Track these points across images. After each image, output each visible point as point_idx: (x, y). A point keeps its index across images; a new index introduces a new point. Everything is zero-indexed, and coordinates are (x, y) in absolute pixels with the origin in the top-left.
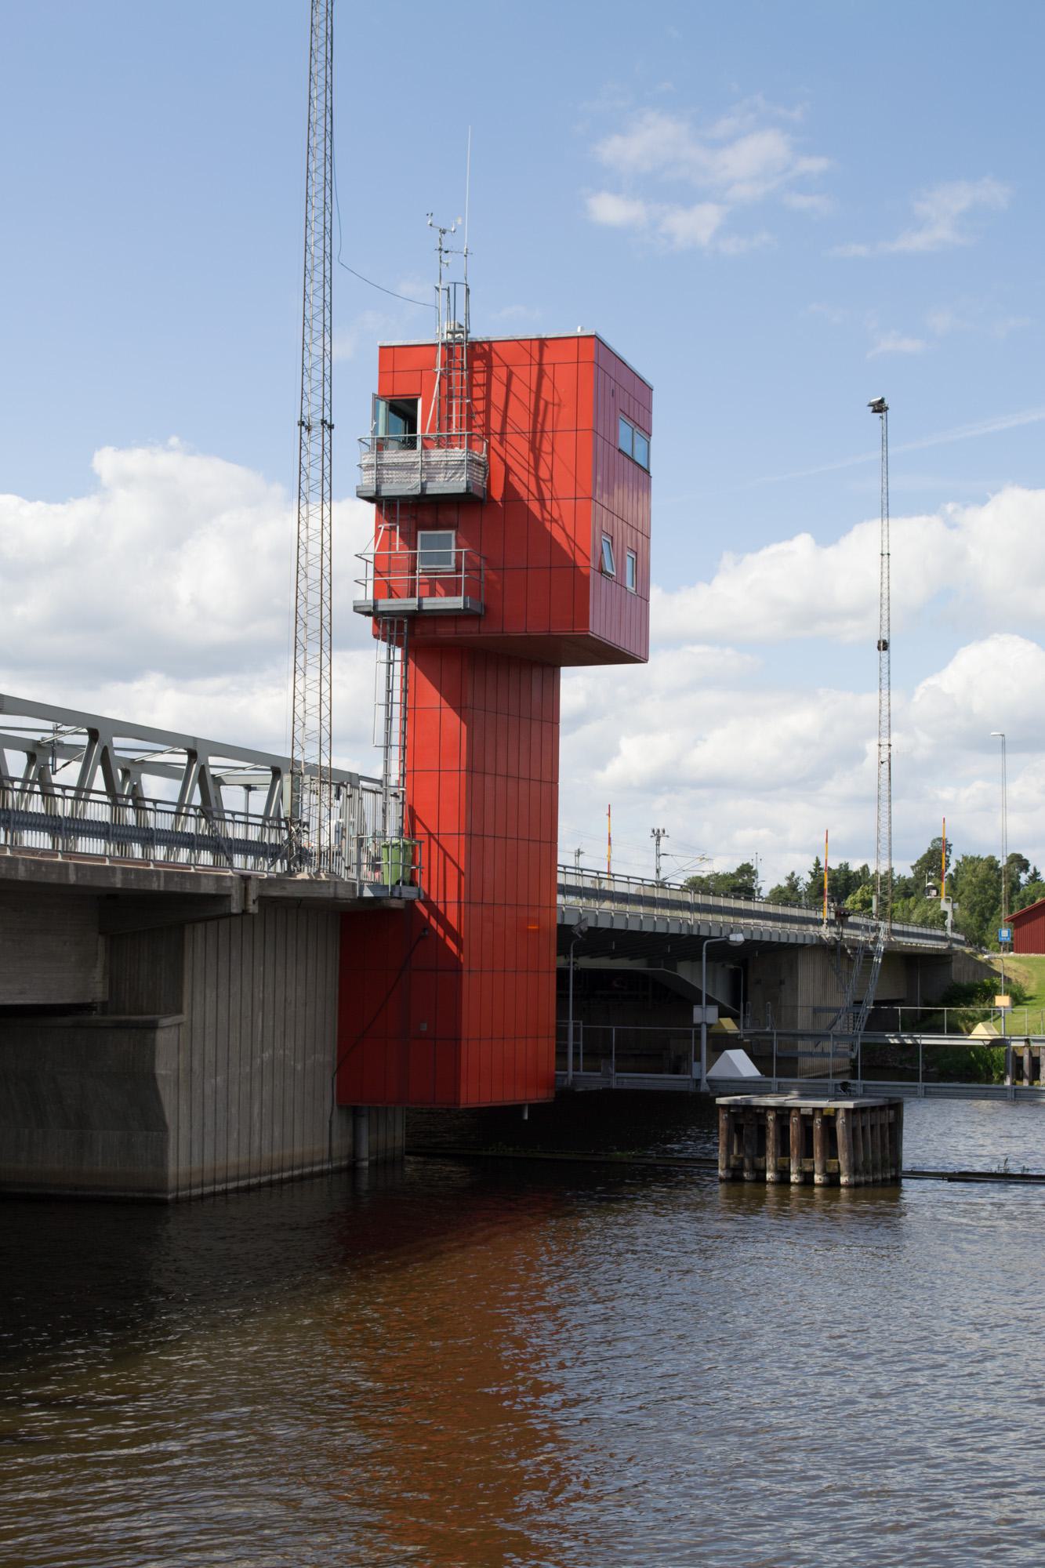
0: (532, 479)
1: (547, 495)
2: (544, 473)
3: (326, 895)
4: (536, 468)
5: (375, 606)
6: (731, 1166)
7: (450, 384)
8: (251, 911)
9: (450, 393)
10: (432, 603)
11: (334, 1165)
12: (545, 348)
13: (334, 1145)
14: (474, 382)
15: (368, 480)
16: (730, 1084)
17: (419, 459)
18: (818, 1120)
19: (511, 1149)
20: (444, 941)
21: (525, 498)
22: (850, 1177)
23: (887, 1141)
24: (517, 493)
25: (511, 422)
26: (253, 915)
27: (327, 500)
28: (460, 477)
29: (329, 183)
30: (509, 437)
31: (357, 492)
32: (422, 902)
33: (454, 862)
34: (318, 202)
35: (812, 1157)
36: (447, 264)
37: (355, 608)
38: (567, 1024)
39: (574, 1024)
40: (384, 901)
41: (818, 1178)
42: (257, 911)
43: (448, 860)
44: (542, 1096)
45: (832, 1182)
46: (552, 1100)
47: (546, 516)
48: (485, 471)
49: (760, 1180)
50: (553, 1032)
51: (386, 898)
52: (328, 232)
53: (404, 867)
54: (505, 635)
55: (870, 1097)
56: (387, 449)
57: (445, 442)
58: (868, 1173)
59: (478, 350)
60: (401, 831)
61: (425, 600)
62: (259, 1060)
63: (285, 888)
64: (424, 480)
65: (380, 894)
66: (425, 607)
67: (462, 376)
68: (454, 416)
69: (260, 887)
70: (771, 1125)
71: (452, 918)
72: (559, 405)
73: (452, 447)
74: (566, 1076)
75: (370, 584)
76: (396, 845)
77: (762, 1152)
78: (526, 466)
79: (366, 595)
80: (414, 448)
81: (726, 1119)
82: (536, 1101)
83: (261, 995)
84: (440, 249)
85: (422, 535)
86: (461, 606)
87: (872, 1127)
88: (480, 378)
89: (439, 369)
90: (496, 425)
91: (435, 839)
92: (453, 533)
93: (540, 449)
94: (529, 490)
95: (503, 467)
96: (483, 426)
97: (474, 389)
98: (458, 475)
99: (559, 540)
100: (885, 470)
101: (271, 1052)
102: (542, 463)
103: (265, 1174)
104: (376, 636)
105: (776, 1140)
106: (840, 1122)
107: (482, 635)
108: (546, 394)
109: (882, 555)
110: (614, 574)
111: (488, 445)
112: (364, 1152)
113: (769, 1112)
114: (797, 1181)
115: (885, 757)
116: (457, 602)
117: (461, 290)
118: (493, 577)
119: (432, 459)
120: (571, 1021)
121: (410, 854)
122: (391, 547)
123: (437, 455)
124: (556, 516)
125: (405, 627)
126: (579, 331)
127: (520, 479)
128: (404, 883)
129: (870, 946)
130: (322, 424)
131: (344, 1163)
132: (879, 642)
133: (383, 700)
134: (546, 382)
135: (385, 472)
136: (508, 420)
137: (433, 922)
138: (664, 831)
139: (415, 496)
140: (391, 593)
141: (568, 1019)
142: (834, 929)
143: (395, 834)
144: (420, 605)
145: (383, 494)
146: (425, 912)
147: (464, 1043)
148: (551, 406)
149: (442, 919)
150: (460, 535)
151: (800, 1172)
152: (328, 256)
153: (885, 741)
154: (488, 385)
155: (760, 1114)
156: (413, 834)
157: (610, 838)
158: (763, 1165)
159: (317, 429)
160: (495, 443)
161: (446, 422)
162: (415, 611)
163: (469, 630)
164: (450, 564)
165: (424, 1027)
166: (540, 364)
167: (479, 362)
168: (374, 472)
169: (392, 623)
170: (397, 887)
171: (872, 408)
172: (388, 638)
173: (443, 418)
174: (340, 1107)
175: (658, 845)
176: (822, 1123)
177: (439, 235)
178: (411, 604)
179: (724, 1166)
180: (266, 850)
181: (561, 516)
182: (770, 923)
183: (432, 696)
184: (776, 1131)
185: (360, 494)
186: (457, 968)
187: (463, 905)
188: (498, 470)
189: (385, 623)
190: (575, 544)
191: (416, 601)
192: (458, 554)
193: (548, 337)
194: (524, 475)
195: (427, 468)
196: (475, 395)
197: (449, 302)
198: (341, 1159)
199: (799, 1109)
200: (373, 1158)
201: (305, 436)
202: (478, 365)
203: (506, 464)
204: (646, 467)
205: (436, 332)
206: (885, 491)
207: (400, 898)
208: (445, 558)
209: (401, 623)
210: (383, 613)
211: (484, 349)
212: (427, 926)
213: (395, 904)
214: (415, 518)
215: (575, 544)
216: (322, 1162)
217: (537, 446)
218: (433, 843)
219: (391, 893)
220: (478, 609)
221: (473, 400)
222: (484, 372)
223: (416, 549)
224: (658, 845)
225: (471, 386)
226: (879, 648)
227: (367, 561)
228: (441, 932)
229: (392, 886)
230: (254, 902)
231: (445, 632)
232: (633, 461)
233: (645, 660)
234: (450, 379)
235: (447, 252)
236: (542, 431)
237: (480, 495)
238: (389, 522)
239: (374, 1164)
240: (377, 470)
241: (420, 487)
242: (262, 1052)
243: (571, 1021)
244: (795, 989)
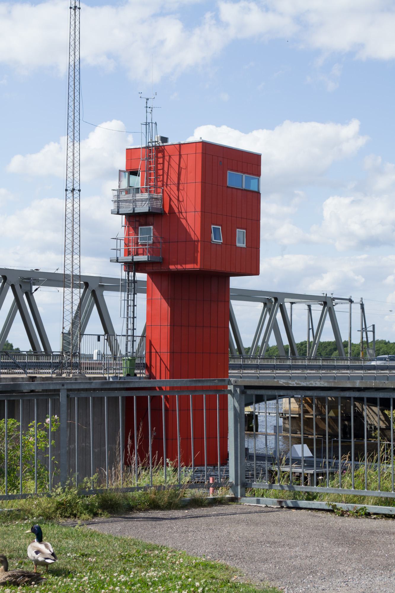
14: (158, 163)
17: (132, 198)
28: (147, 205)
54: (170, 270)
61: (135, 257)
66: (134, 260)
84: (147, 107)
85: (141, 228)
86: (146, 260)
88: (160, 161)
91: (158, 354)
92: (152, 227)
95: (168, 199)
98: (146, 204)
107: (162, 270)
111: (163, 190)
130: (66, 191)
144: (133, 259)
154: (163, 163)
164: (151, 240)
168: (117, 204)
188: (167, 199)
202: (160, 155)
205: (141, 144)
211: (162, 148)
220: (157, 259)
237: (159, 212)
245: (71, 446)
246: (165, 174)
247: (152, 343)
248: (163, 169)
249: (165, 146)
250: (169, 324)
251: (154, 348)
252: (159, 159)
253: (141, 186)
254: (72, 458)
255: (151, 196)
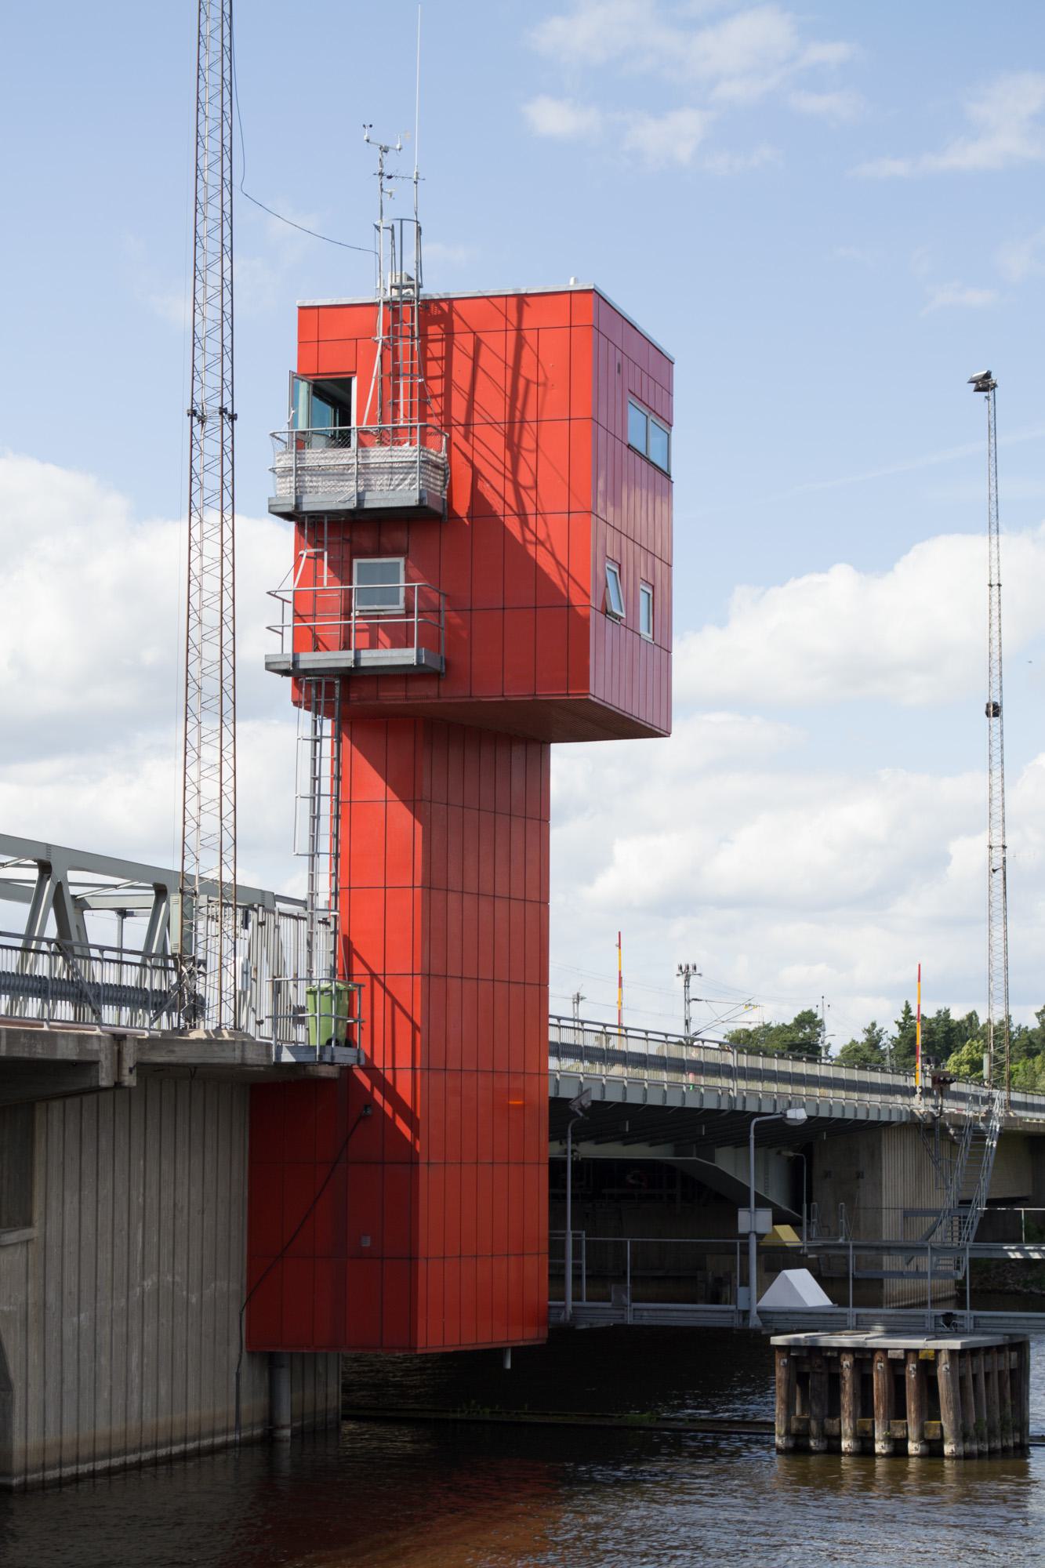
0: (509, 486)
1: (530, 508)
2: (525, 478)
3: (230, 1061)
4: (515, 471)
5: (295, 663)
6: (793, 1431)
7: (396, 358)
8: (126, 1084)
9: (396, 368)
10: (372, 658)
11: (243, 1435)
12: (525, 306)
13: (244, 1406)
14: (429, 355)
15: (285, 492)
16: (790, 1317)
17: (355, 461)
18: (912, 1367)
19: (488, 1410)
20: (393, 1120)
21: (500, 512)
22: (957, 1445)
23: (1008, 1395)
24: (490, 506)
25: (481, 411)
26: (130, 1088)
27: (228, 721)
29: (228, 85)
30: (477, 429)
31: (270, 506)
32: (363, 1068)
33: (405, 1012)
34: (212, 111)
35: (904, 1417)
36: (391, 194)
37: (267, 664)
38: (564, 1235)
39: (574, 1235)
40: (311, 1068)
41: (913, 1447)
42: (134, 1084)
43: (397, 1009)
44: (529, 1335)
45: (933, 1450)
46: (544, 1342)
47: (529, 536)
48: (445, 475)
49: (834, 1450)
50: (544, 1247)
51: (313, 1064)
52: (227, 151)
53: (337, 1020)
54: (474, 700)
55: (984, 1333)
56: (310, 447)
57: (390, 437)
58: (982, 1439)
59: (434, 310)
60: (333, 971)
61: (364, 654)
62: (138, 1289)
63: (173, 1052)
64: (361, 489)
65: (304, 1058)
66: (363, 663)
67: (412, 346)
68: (402, 401)
69: (140, 1049)
70: (847, 1373)
71: (404, 1090)
72: (545, 385)
73: (400, 443)
74: (564, 1307)
75: (288, 633)
76: (327, 990)
77: (835, 1411)
78: (501, 468)
79: (282, 647)
80: (347, 445)
81: (785, 1366)
82: (522, 1344)
83: (141, 1200)
84: (381, 174)
85: (359, 564)
86: (413, 661)
87: (987, 1375)
88: (436, 349)
89: (380, 337)
90: (459, 411)
91: (379, 981)
92: (401, 561)
93: (519, 446)
94: (505, 502)
95: (471, 470)
96: (441, 414)
97: (429, 363)
98: (407, 482)
99: (547, 570)
100: (993, 470)
101: (155, 1278)
102: (522, 465)
103: (147, 1448)
104: (296, 703)
105: (854, 1394)
106: (943, 1369)
108: (528, 370)
109: (991, 585)
110: (623, 615)
111: (449, 440)
112: (285, 1416)
113: (843, 1356)
114: (884, 1451)
115: (997, 863)
116: (407, 656)
117: (410, 229)
118: (457, 621)
119: (372, 461)
120: (570, 1232)
121: (345, 1002)
122: (317, 581)
123: (378, 454)
124: (542, 536)
125: (337, 690)
126: (571, 285)
127: (492, 486)
128: (338, 1043)
129: (981, 1124)
130: (221, 413)
131: (258, 1431)
132: (988, 706)
133: (307, 792)
134: (527, 356)
135: (307, 478)
136: (476, 406)
137: (378, 1096)
138: (695, 968)
139: (349, 511)
140: (317, 645)
141: (565, 1228)
142: (931, 1101)
143: (324, 975)
145: (305, 508)
146: (366, 1082)
147: (422, 1263)
148: (533, 387)
149: (389, 1091)
150: (410, 563)
151: (889, 1439)
152: (227, 184)
153: (997, 841)
154: (448, 358)
155: (831, 1358)
156: (349, 975)
157: (620, 978)
158: (836, 1429)
159: (214, 421)
160: (457, 435)
161: (390, 410)
162: (349, 668)
163: (424, 693)
164: (398, 603)
165: (367, 1242)
166: (519, 329)
167: (436, 326)
168: (293, 478)
169: (319, 684)
170: (328, 1048)
171: (974, 385)
172: (313, 705)
173: (388, 405)
174: (251, 1353)
175: (687, 986)
176: (917, 1370)
177: (379, 154)
178: (343, 659)
179: (783, 1432)
180: (147, 999)
181: (548, 536)
182: (843, 1094)
183: (373, 785)
184: (854, 1384)
185: (273, 509)
186: (412, 1161)
187: (419, 1072)
188: (464, 475)
189: (309, 685)
190: (569, 574)
191: (351, 654)
192: (409, 591)
193: (529, 292)
194: (498, 482)
195: (364, 471)
196: (429, 374)
197: (394, 246)
198: (252, 1425)
199: (885, 1351)
200: (297, 1424)
201: (197, 429)
202: (433, 330)
203: (473, 466)
204: (665, 470)
206: (993, 498)
207: (332, 1064)
208: (390, 596)
209: (330, 685)
210: (307, 672)
211: (440, 308)
212: (371, 1103)
213: (325, 1071)
214: (350, 541)
215: (569, 574)
216: (226, 1431)
217: (516, 440)
218: (376, 985)
219: (320, 1056)
220: (436, 665)
221: (427, 378)
222: (442, 340)
223: (351, 584)
224: (687, 986)
225: (424, 360)
226: (987, 714)
227: (284, 600)
228: (388, 1109)
229: (322, 1048)
230: (131, 1070)
231: (393, 696)
232: (647, 460)
233: (666, 734)
234: (395, 350)
235: (390, 177)
236: (522, 422)
237: (439, 508)
238: (314, 547)
239: (299, 1434)
240: (297, 476)
241: (355, 498)
242: (143, 1278)
243: (570, 1232)
244: (878, 1185)
245: (145, 1284)
246: (454, 393)
247: (354, 947)
248: (447, 376)
249: (455, 302)
250: (418, 883)
251: (361, 959)
252: (429, 345)
253: (367, 424)
254: (148, 1326)
255: (426, 454)
